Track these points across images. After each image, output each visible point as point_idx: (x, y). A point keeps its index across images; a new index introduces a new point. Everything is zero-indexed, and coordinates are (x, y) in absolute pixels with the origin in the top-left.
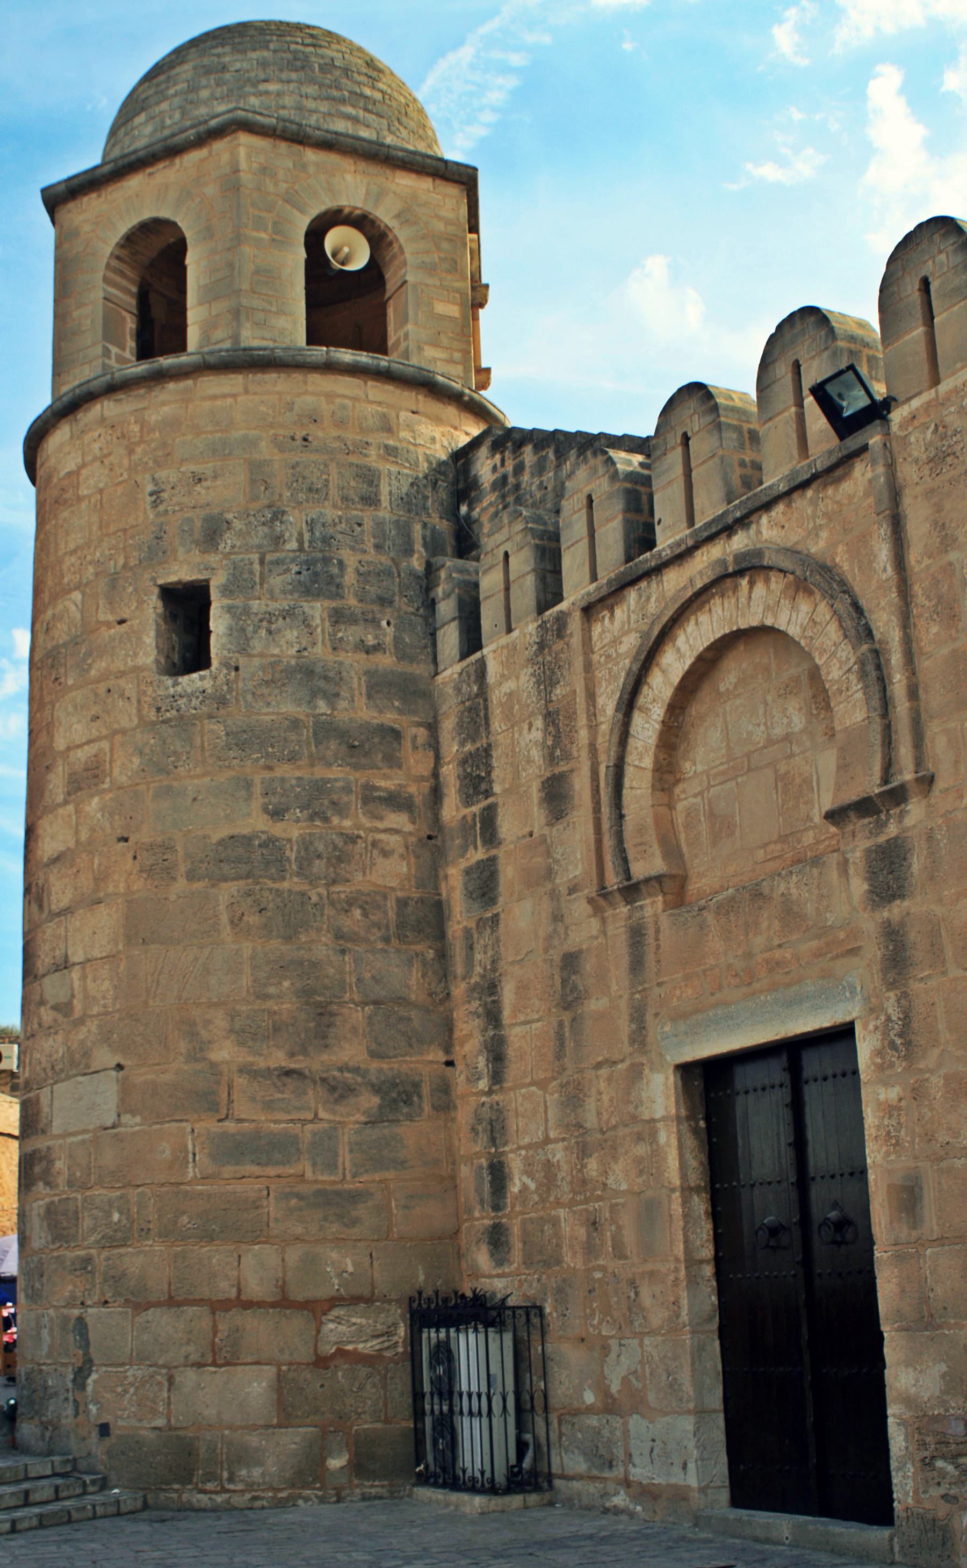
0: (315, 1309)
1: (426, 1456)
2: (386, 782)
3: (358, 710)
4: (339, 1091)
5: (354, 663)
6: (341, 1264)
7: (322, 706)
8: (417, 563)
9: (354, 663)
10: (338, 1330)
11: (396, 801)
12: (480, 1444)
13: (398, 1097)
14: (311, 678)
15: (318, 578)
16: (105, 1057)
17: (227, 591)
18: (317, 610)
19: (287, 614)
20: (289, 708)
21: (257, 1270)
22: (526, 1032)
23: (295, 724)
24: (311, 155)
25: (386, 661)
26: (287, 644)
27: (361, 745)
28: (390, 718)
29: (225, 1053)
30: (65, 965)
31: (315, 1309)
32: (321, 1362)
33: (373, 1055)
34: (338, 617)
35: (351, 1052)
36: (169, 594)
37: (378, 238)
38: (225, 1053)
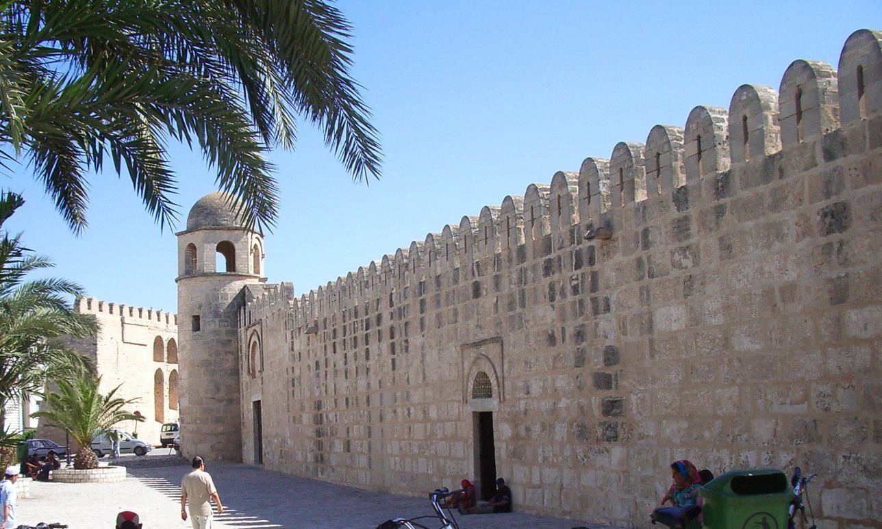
2: (229, 349)
4: (220, 401)
5: (223, 329)
7: (218, 337)
8: (235, 310)
9: (223, 329)
14: (216, 332)
16: (187, 395)
17: (202, 317)
18: (217, 320)
19: (212, 321)
20: (212, 338)
23: (213, 340)
24: (217, 231)
25: (229, 328)
26: (212, 327)
28: (230, 338)
30: (181, 379)
33: (226, 395)
34: (220, 321)
36: (194, 316)
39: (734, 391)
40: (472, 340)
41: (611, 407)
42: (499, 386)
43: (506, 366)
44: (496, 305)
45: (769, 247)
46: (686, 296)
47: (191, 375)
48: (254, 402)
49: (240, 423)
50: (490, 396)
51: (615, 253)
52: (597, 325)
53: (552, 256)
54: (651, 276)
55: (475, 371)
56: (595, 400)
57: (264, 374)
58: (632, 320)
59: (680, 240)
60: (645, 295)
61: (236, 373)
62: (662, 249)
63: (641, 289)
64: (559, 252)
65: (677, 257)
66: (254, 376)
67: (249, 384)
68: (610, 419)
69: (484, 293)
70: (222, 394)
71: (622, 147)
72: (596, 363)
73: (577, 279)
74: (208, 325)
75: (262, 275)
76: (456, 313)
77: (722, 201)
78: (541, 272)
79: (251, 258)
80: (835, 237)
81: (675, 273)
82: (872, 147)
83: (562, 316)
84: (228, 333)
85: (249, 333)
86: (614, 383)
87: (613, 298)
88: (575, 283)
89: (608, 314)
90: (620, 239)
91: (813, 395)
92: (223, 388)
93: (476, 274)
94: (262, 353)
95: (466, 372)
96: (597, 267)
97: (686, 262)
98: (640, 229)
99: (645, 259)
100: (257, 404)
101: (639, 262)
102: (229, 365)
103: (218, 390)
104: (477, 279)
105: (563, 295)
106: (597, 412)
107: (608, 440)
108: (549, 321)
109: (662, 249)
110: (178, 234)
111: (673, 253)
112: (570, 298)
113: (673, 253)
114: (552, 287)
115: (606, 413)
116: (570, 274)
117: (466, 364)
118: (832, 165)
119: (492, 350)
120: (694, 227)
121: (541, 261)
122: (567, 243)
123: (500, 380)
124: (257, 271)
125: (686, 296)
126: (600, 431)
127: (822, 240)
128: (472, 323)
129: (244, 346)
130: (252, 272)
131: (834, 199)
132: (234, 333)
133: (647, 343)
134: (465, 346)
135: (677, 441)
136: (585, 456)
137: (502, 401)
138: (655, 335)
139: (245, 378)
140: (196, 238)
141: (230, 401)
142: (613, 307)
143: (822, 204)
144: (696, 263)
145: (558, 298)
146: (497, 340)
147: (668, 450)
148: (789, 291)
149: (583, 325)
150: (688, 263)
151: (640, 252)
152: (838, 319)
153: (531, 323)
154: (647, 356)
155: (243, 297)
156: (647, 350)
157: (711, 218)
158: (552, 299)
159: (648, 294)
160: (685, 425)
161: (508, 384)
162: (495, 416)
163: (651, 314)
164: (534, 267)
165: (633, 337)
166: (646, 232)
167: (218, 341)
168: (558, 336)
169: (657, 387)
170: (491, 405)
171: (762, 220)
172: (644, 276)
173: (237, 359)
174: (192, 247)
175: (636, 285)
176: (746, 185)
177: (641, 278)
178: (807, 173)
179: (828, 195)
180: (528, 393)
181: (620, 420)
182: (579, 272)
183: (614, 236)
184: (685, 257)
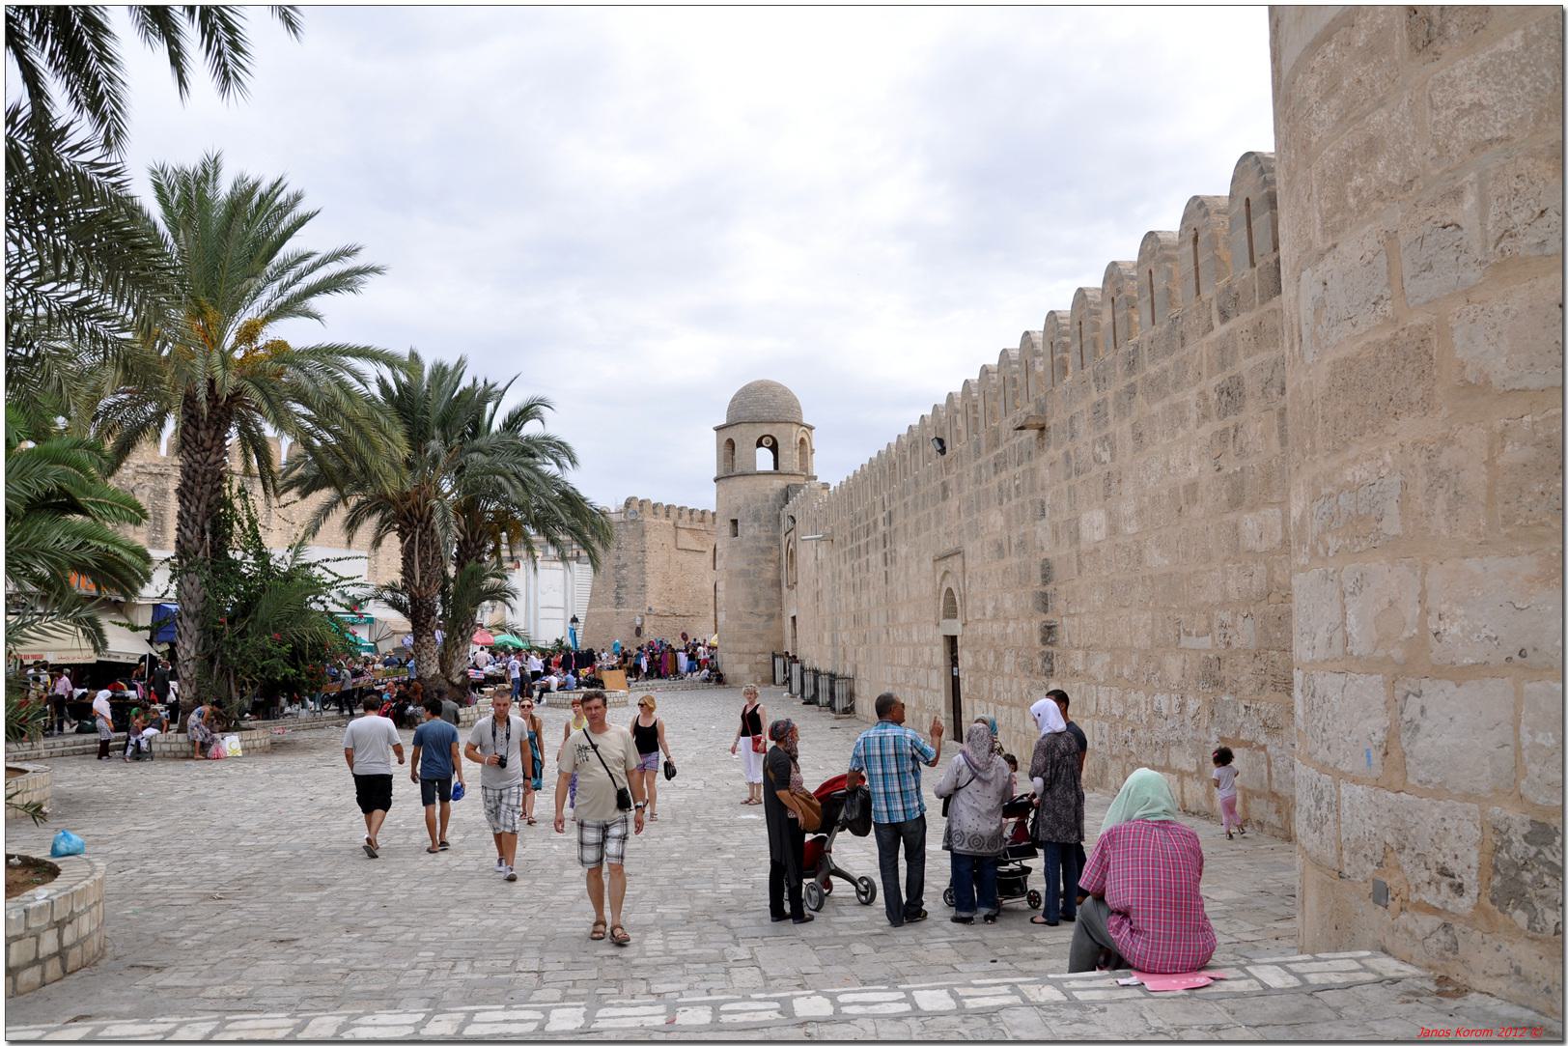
3: (764, 544)
10: (759, 658)
13: (771, 617)
15: (756, 518)
27: (763, 551)
39: (1146, 617)
41: (1048, 631)
45: (1174, 435)
46: (1106, 497)
54: (1078, 472)
61: (778, 584)
65: (1098, 449)
68: (1049, 649)
70: (762, 608)
71: (1052, 315)
74: (748, 530)
77: (1133, 379)
80: (1231, 420)
81: (1096, 469)
82: (1262, 303)
84: (768, 539)
91: (1216, 625)
92: (763, 602)
102: (769, 574)
103: (756, 603)
110: (718, 429)
115: (1044, 641)
118: (1226, 327)
127: (1219, 426)
131: (1228, 373)
138: (1083, 546)
140: (731, 433)
141: (771, 617)
143: (1217, 380)
148: (1192, 488)
150: (1106, 457)
152: (1236, 527)
157: (1125, 398)
158: (1001, 503)
163: (1078, 519)
168: (1006, 546)
170: (954, 627)
171: (1167, 401)
173: (779, 568)
174: (731, 443)
176: (1152, 361)
177: (1069, 476)
178: (1205, 340)
179: (1223, 366)
182: (1020, 469)
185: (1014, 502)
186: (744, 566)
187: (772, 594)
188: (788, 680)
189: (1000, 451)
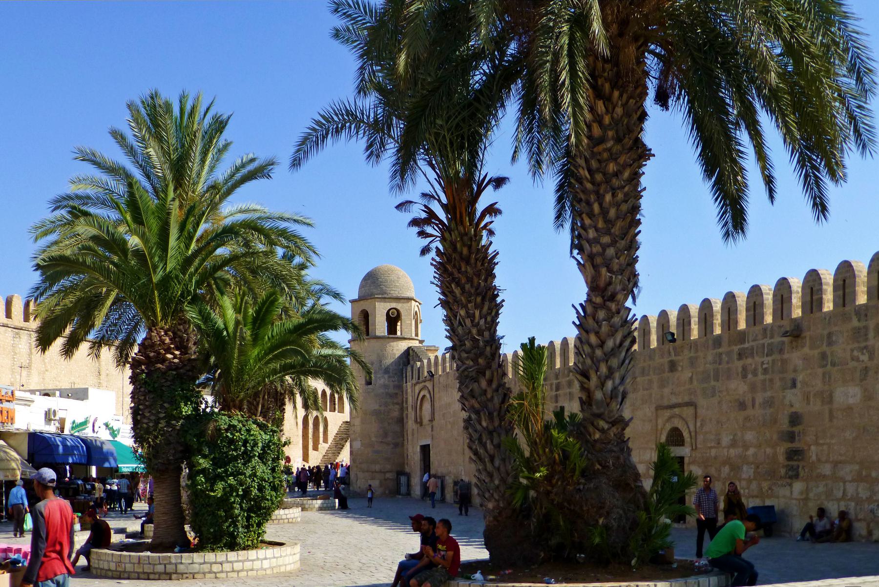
0: (385, 473)
1: (398, 492)
3: (392, 391)
4: (388, 444)
6: (388, 467)
9: (391, 384)
10: (388, 475)
11: (397, 404)
12: (403, 489)
14: (385, 386)
18: (386, 376)
21: (377, 467)
22: (410, 438)
26: (382, 381)
29: (373, 439)
31: (385, 473)
32: (385, 480)
34: (389, 377)
35: (389, 439)
37: (398, 311)
38: (373, 439)
40: (666, 403)
41: (794, 454)
42: (691, 438)
43: (698, 424)
44: (691, 378)
46: (861, 380)
47: (363, 422)
48: (421, 446)
49: (404, 464)
50: (683, 445)
51: (803, 347)
52: (784, 397)
53: (746, 345)
55: (668, 427)
56: (781, 450)
57: (434, 423)
58: (815, 395)
59: (858, 342)
60: (826, 378)
61: (401, 421)
62: (842, 348)
63: (824, 374)
64: (751, 343)
65: (856, 353)
66: (421, 424)
67: (415, 431)
69: (680, 369)
72: (784, 424)
73: (768, 363)
75: (420, 338)
76: (650, 382)
78: (736, 357)
79: (413, 322)
81: (853, 364)
83: (753, 388)
84: (396, 387)
85: (417, 388)
86: (797, 438)
87: (800, 378)
88: (765, 366)
89: (793, 390)
90: (808, 338)
93: (673, 353)
94: (433, 405)
95: (659, 427)
96: (786, 356)
97: (862, 358)
98: (825, 332)
99: (829, 353)
100: (425, 449)
101: (824, 356)
102: (396, 414)
104: (673, 358)
105: (755, 374)
106: (781, 459)
107: (791, 477)
108: (741, 392)
109: (842, 348)
111: (852, 350)
112: (761, 377)
113: (852, 350)
114: (744, 369)
116: (762, 359)
117: (660, 421)
119: (688, 412)
120: (871, 334)
121: (736, 348)
122: (760, 337)
123: (693, 434)
124: (417, 335)
125: (861, 380)
126: (783, 471)
128: (667, 391)
129: (410, 399)
130: (413, 335)
132: (400, 387)
133: (827, 412)
134: (659, 408)
135: (849, 478)
136: (770, 489)
137: (694, 449)
139: (411, 424)
141: (396, 445)
142: (799, 385)
144: (871, 358)
145: (750, 376)
146: (691, 404)
147: (841, 484)
149: (773, 397)
150: (865, 358)
151: (824, 348)
153: (725, 393)
154: (827, 420)
155: (409, 356)
156: (827, 416)
158: (744, 376)
159: (830, 378)
160: (857, 467)
161: (700, 438)
162: (686, 460)
164: (729, 354)
165: (816, 406)
166: (830, 335)
167: (387, 394)
168: (749, 404)
169: (833, 441)
172: (826, 365)
173: (402, 410)
175: (820, 371)
180: (719, 443)
181: (801, 464)
182: (770, 359)
183: (803, 335)
184: (863, 354)
185: (761, 377)
186: (377, 407)
187: (397, 428)
188: (408, 494)
189: (746, 345)
